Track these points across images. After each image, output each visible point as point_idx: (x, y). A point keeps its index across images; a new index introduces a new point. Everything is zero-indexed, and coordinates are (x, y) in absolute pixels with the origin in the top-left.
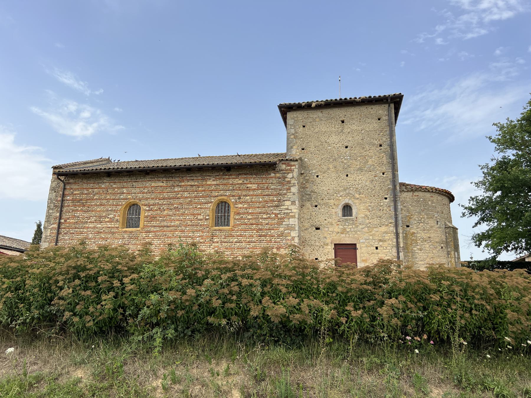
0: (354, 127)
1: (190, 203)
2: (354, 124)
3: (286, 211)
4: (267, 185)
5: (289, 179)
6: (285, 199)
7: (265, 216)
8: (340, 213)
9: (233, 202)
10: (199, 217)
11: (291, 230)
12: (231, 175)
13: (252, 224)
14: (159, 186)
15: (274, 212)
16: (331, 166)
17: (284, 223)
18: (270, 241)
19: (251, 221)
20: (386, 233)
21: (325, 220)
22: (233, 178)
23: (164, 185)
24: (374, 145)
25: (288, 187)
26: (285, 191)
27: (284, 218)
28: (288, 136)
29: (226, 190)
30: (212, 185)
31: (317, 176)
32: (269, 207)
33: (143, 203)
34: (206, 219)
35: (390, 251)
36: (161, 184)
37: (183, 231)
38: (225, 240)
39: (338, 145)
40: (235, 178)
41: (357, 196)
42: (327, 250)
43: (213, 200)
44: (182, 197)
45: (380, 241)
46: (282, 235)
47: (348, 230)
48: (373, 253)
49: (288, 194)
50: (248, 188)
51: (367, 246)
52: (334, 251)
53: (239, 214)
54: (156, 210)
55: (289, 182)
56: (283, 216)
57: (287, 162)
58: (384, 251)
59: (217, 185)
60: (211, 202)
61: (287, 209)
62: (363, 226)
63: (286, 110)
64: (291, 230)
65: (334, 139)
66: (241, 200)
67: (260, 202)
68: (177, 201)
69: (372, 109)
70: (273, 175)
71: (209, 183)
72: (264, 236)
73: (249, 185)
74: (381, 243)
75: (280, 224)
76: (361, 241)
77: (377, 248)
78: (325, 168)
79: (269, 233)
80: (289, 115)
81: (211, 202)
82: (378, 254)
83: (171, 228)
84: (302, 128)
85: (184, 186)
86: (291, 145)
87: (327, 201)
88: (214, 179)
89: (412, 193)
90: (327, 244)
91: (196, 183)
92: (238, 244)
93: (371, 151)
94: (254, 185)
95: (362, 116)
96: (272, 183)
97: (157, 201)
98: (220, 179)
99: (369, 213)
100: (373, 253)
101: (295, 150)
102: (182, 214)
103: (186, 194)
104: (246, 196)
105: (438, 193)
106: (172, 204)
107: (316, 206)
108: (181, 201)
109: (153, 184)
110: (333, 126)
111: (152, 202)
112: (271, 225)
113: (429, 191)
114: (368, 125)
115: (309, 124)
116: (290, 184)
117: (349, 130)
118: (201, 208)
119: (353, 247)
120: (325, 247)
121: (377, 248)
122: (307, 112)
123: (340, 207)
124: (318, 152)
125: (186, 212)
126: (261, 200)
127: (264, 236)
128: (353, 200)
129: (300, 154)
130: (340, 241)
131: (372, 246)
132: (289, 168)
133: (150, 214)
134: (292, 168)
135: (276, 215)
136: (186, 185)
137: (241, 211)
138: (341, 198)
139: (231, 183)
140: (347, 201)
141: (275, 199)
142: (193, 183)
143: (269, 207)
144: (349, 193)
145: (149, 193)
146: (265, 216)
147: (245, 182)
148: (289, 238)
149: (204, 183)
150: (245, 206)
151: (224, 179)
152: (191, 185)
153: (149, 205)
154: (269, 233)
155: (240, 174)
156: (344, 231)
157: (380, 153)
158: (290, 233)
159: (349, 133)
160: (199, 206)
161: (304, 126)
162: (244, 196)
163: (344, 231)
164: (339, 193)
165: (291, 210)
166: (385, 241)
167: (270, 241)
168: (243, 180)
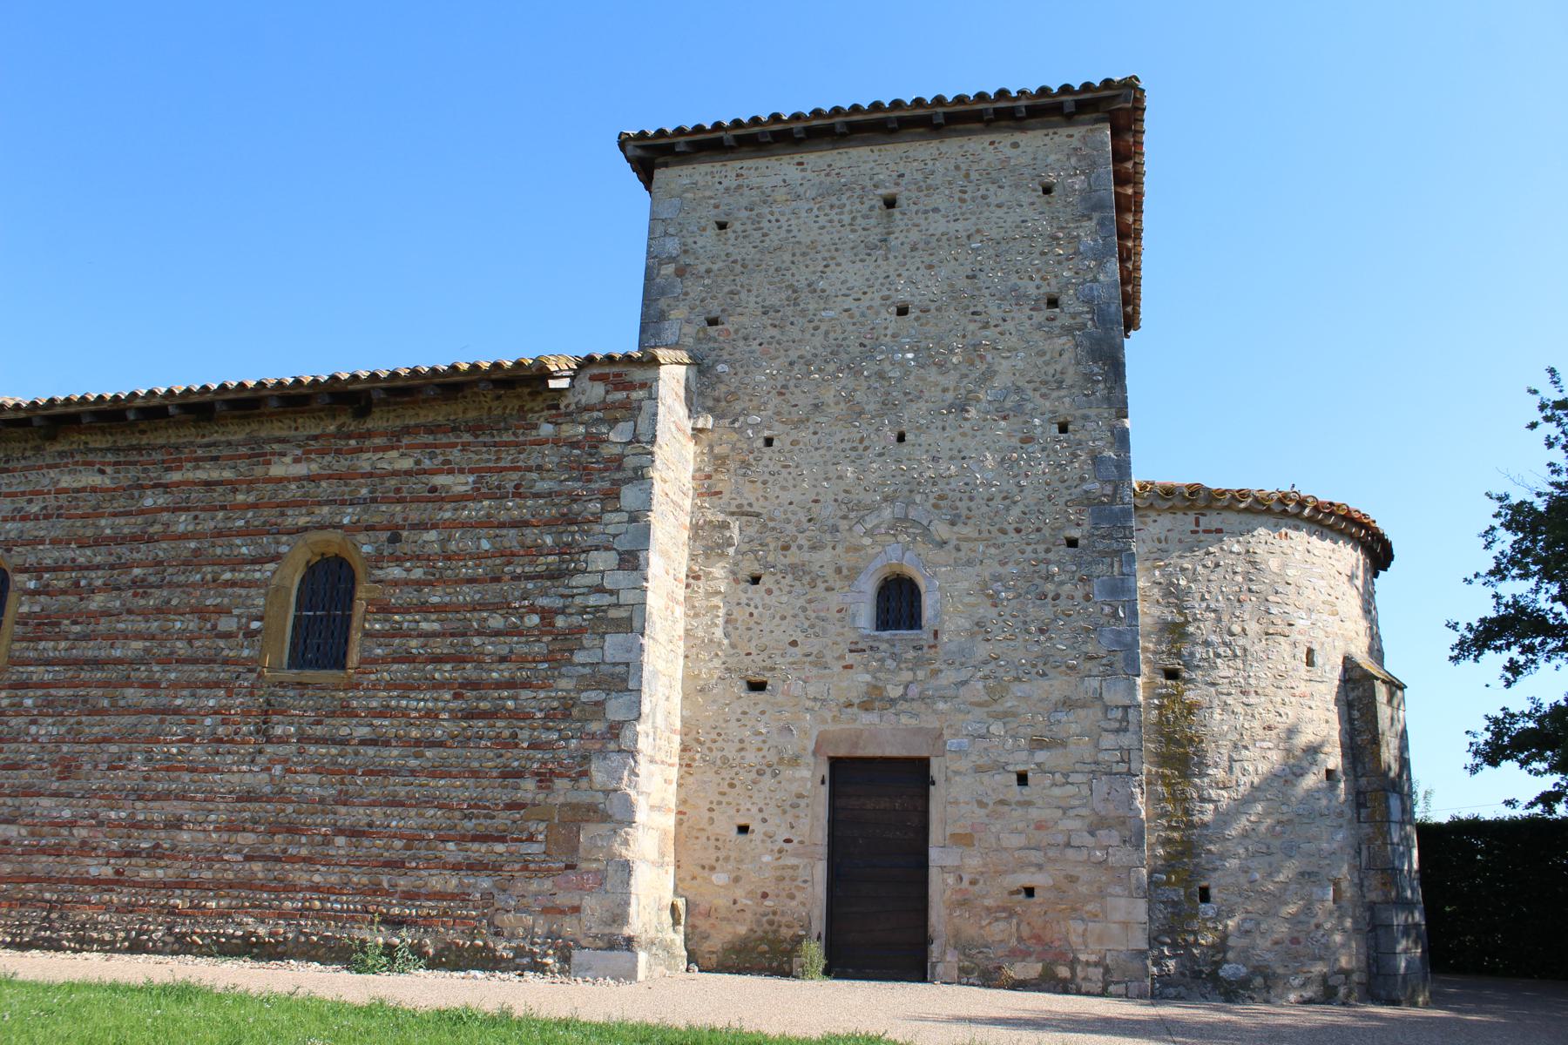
0: (939, 225)
1: (192, 562)
2: (936, 210)
3: (593, 600)
4: (515, 476)
5: (617, 450)
6: (590, 541)
7: (496, 622)
8: (865, 613)
9: (368, 558)
10: (227, 624)
11: (608, 691)
12: (369, 434)
13: (438, 660)
14: (84, 489)
15: (543, 602)
16: (828, 396)
17: (579, 657)
18: (512, 742)
19: (441, 647)
20: (1068, 704)
21: (794, 644)
22: (376, 449)
23: (108, 482)
24: (1019, 298)
25: (607, 485)
26: (595, 506)
27: (581, 630)
28: (648, 268)
29: (343, 503)
30: (288, 480)
31: (769, 442)
32: (516, 578)
33: (18, 561)
34: (250, 634)
35: (1085, 791)
36: (97, 480)
37: (151, 685)
38: (319, 730)
39: (865, 302)
40: (385, 449)
41: (941, 530)
42: (795, 788)
43: (284, 549)
44: (166, 536)
45: (1038, 743)
46: (565, 710)
47: (894, 692)
48: (1002, 802)
49: (607, 517)
50: (433, 489)
51: (979, 770)
52: (824, 791)
53: (385, 609)
54: (64, 592)
55: (617, 462)
56: (576, 620)
57: (615, 370)
58: (1057, 791)
59: (311, 478)
60: (276, 558)
61: (600, 589)
62: (964, 674)
63: (650, 155)
64: (608, 691)
65: (851, 273)
66: (400, 548)
67: (479, 557)
68: (143, 552)
69: (1015, 145)
70: (546, 430)
71: (276, 470)
72: (483, 715)
73: (439, 480)
74: (1041, 756)
75: (557, 660)
76: (952, 743)
77: (1022, 779)
78: (805, 402)
79: (510, 703)
80: (660, 175)
81: (276, 558)
82: (1028, 804)
83: (113, 674)
84: (712, 231)
85: (178, 484)
86: (663, 303)
87: (806, 556)
88: (299, 452)
89: (1191, 517)
90: (795, 761)
91: (228, 474)
92: (371, 751)
93: (1009, 326)
94: (461, 478)
95: (974, 176)
96: (539, 468)
97: (69, 554)
98: (322, 453)
99: (993, 612)
100: (1002, 802)
101: (676, 327)
102: (161, 611)
103: (183, 523)
104: (422, 526)
105: (1310, 520)
106: (128, 566)
107: (755, 580)
108: (162, 550)
109: (66, 481)
110: (846, 219)
111: (49, 555)
112: (523, 659)
113: (1269, 511)
114: (1000, 212)
115: (744, 214)
116: (619, 468)
117: (914, 235)
118: (233, 584)
119: (912, 775)
120: (788, 773)
121: (1022, 779)
122: (738, 164)
123: (868, 586)
124: (775, 332)
125: (174, 602)
126: (485, 545)
127: (483, 715)
128: (921, 548)
129: (699, 340)
130: (855, 745)
131: (1003, 768)
132: (620, 395)
133: (37, 609)
134: (635, 395)
135: (547, 615)
136: (186, 483)
137: (396, 597)
138: (867, 541)
139: (367, 467)
140: (897, 556)
141: (549, 540)
142: (215, 475)
143: (516, 578)
144: (906, 519)
145: (47, 517)
146: (496, 622)
147: (427, 464)
148: (596, 727)
149: (259, 471)
150: (418, 573)
151: (338, 452)
152: (209, 484)
153: (37, 571)
154: (510, 703)
155: (407, 430)
156: (873, 700)
157: (1049, 336)
158: (599, 704)
159: (914, 249)
160: (227, 576)
161: (722, 226)
162: (414, 527)
163: (873, 700)
164: (861, 520)
165: (611, 592)
166: (1063, 744)
167: (512, 742)
168: (417, 453)
